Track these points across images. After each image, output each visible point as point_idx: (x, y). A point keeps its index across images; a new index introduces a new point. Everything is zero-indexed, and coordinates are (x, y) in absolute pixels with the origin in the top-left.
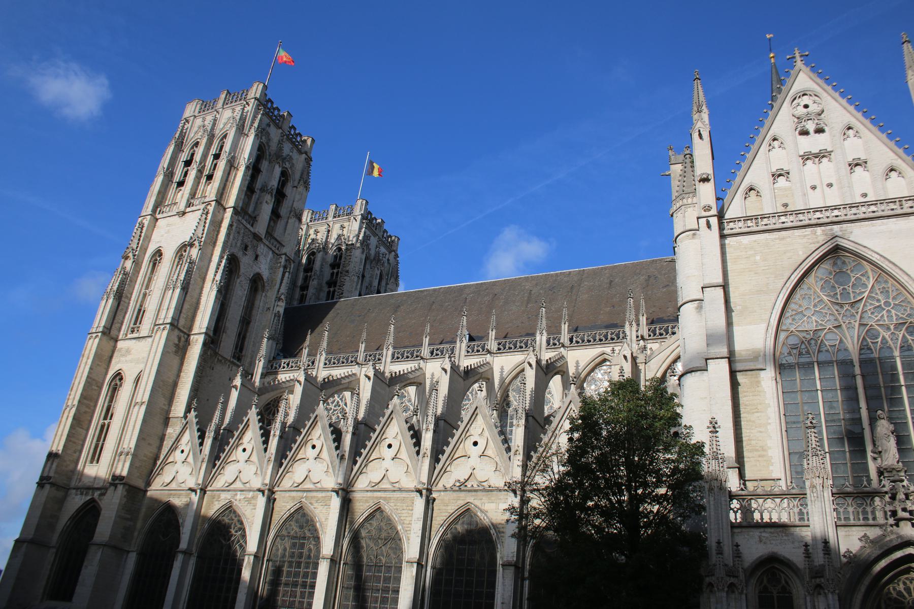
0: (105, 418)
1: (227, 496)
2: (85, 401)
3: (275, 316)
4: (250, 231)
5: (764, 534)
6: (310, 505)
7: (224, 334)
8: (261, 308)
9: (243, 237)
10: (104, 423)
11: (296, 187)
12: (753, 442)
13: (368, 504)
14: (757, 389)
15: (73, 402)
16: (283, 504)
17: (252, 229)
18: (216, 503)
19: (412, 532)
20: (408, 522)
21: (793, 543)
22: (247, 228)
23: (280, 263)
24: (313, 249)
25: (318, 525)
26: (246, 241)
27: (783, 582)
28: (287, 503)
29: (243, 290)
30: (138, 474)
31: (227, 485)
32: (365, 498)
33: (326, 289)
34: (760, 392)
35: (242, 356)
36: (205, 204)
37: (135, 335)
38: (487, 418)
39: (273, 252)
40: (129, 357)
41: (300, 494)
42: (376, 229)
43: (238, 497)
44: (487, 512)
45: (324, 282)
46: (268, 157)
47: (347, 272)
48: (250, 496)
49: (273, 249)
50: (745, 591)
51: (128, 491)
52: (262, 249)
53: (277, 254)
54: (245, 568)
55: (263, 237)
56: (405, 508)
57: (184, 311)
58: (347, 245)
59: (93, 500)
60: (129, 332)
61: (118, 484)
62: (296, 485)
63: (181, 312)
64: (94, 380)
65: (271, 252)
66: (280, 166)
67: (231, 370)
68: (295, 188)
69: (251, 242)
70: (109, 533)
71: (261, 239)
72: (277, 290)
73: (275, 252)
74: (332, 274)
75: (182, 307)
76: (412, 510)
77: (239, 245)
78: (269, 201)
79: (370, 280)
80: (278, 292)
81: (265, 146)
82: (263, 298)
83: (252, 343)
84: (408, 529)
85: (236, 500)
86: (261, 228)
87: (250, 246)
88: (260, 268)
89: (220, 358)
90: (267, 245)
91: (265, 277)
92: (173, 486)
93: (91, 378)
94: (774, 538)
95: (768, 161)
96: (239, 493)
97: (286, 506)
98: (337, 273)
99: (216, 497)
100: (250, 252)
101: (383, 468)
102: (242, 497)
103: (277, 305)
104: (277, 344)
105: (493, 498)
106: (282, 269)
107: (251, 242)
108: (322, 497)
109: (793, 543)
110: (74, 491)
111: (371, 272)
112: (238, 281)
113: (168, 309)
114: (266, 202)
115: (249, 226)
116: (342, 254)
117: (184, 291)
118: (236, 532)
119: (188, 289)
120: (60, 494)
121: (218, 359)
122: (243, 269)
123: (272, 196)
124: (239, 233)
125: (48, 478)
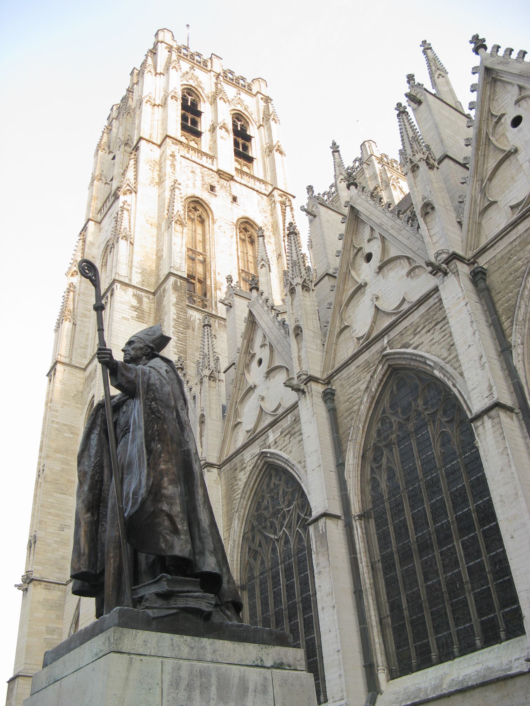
4: (211, 170)
6: (402, 350)
7: (218, 291)
16: (352, 389)
25: (436, 373)
28: (358, 381)
54: (317, 553)
55: (233, 173)
64: (66, 425)
68: (262, 127)
69: (218, 182)
81: (196, 89)
99: (239, 465)
108: (422, 316)
114: (222, 138)
117: (126, 240)
123: (227, 131)
124: (193, 172)
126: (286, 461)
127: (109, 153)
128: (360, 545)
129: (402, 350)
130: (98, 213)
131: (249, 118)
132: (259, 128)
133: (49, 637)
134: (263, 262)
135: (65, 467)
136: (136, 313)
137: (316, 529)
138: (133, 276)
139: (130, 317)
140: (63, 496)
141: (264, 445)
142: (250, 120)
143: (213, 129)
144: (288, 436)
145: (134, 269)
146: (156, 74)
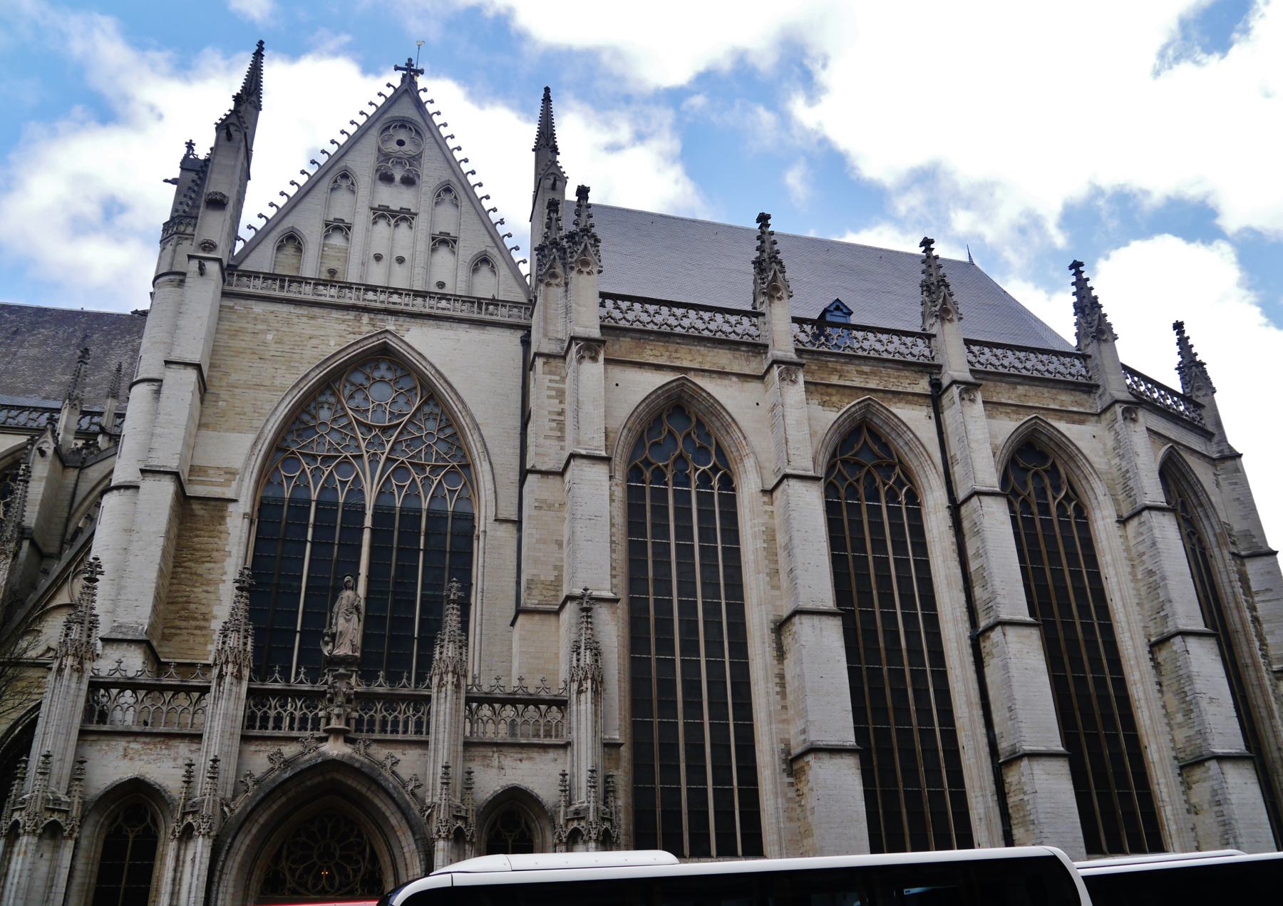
5: (133, 745)
12: (192, 606)
14: (219, 527)
21: (175, 759)
27: (149, 819)
34: (221, 532)
50: (75, 835)
94: (148, 751)
95: (328, 205)
109: (175, 759)
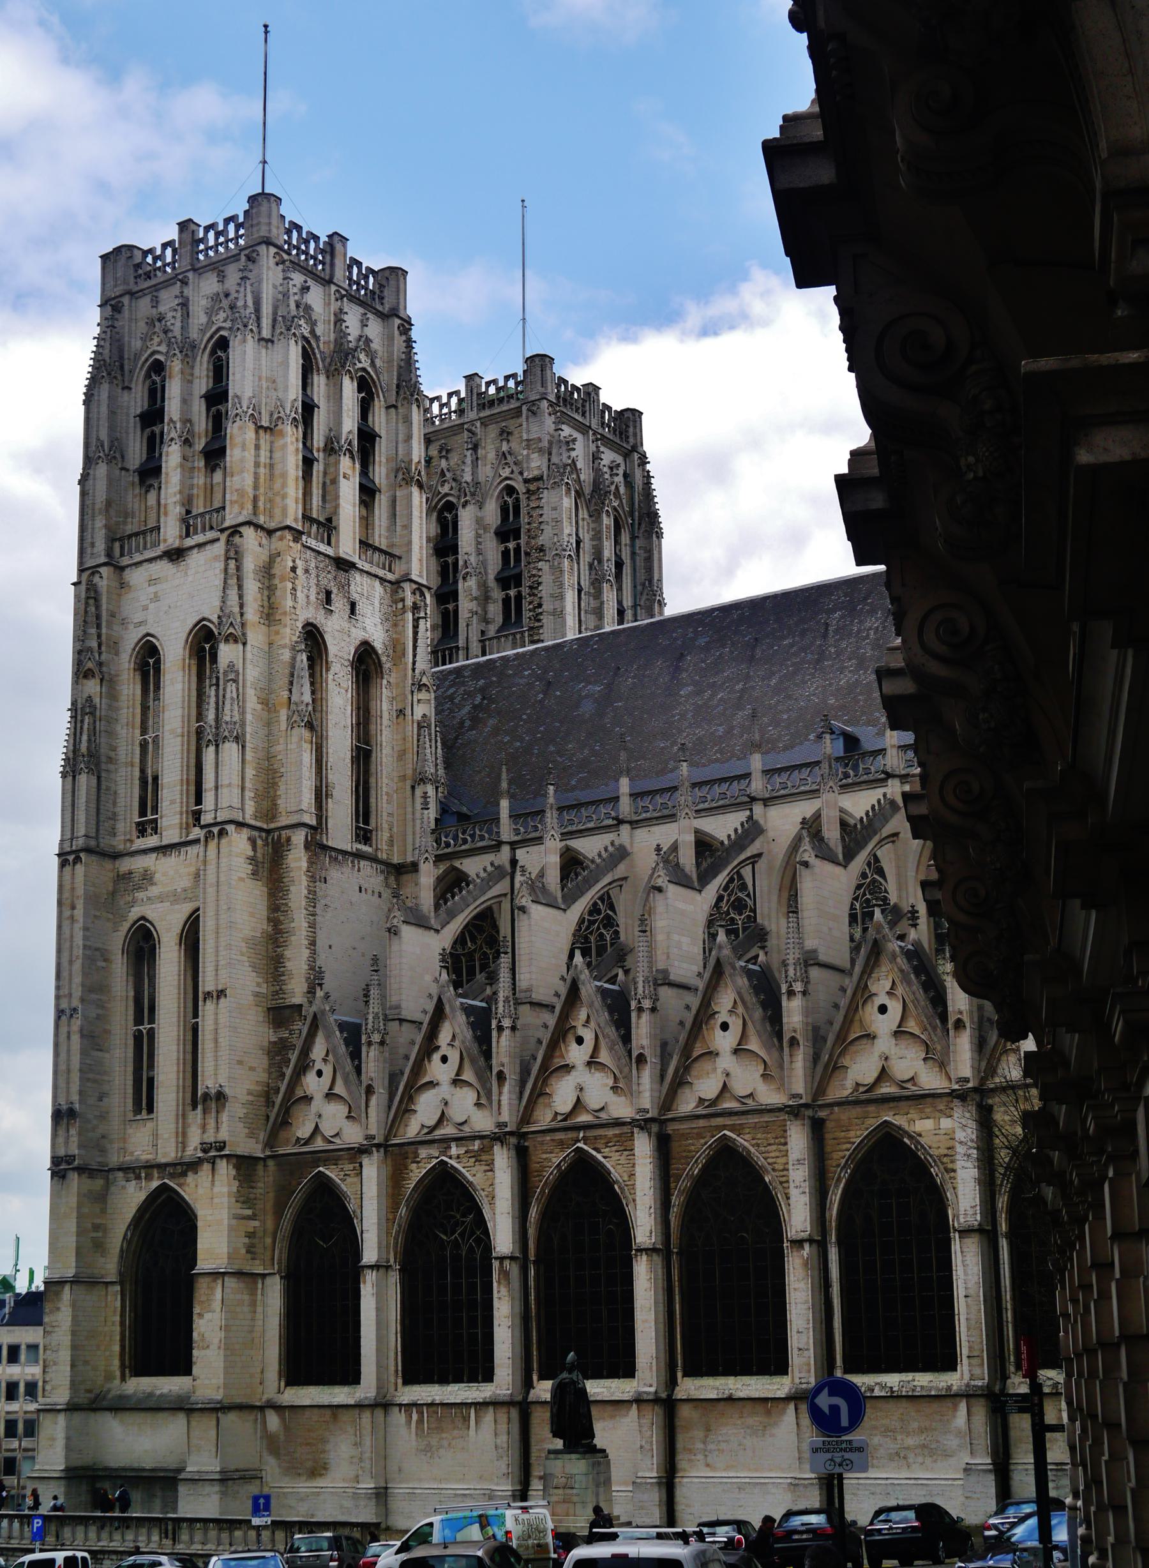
0: (139, 1020)
1: (431, 1151)
2: (94, 996)
3: (420, 727)
6: (594, 1153)
7: (330, 800)
8: (385, 715)
9: (318, 576)
10: (140, 1031)
11: (395, 407)
13: (703, 1141)
15: (70, 1002)
16: (545, 1156)
17: (330, 551)
18: (414, 1166)
19: (792, 1185)
20: (781, 1167)
22: (319, 553)
23: (403, 600)
24: (447, 495)
25: (616, 1187)
26: (324, 582)
29: (343, 691)
30: (247, 1131)
31: (426, 1130)
32: (695, 1131)
33: (497, 594)
35: (371, 831)
36: (227, 533)
37: (152, 841)
38: (899, 960)
39: (382, 580)
40: (154, 891)
41: (571, 1135)
42: (583, 414)
43: (454, 1151)
44: (920, 1135)
45: (491, 577)
46: (321, 366)
47: (541, 549)
48: (476, 1148)
49: (381, 573)
51: (237, 1167)
52: (360, 585)
53: (390, 582)
54: (499, 1282)
55: (356, 559)
56: (772, 1141)
57: (248, 785)
58: (526, 481)
59: (164, 1188)
60: (135, 833)
61: (215, 1157)
62: (559, 1118)
63: (243, 789)
64: (97, 949)
65: (377, 583)
66: (352, 378)
67: (359, 870)
68: (393, 410)
70: (225, 1250)
71: (353, 565)
72: (410, 666)
73: (385, 581)
74: (505, 554)
75: (243, 779)
76: (786, 1144)
77: (313, 598)
78: (349, 472)
79: (594, 547)
80: (414, 670)
82: (384, 690)
83: (385, 797)
84: (783, 1179)
85: (450, 1158)
86: (347, 545)
87: (335, 590)
88: (364, 629)
89: (333, 854)
90: (367, 573)
91: (378, 646)
92: (319, 1144)
93: (90, 948)
96: (453, 1145)
97: (550, 1160)
98: (518, 549)
99: (411, 1156)
100: (339, 604)
101: (719, 1071)
102: (462, 1151)
103: (419, 701)
104: (437, 788)
105: (928, 1110)
106: (410, 616)
107: (335, 578)
108: (615, 1135)
110: (120, 1174)
111: (592, 525)
112: (330, 677)
113: (217, 788)
115: (323, 548)
116: (518, 500)
118: (464, 1216)
119: (244, 735)
120: (99, 1183)
121: (330, 857)
122: (332, 649)
123: (352, 458)
125: (69, 1159)
126: (471, 1183)
127: (123, 389)
128: (532, 1283)
129: (594, 1153)
130: (114, 540)
131: (374, 382)
132: (388, 408)
133: (95, 1235)
134: (426, 855)
135: (100, 1012)
136: (251, 867)
137: (501, 1264)
138: (247, 807)
139: (244, 876)
140: (100, 1054)
141: (444, 1153)
142: (376, 387)
143: (331, 449)
144: (473, 1160)
145: (249, 794)
146: (261, 339)
